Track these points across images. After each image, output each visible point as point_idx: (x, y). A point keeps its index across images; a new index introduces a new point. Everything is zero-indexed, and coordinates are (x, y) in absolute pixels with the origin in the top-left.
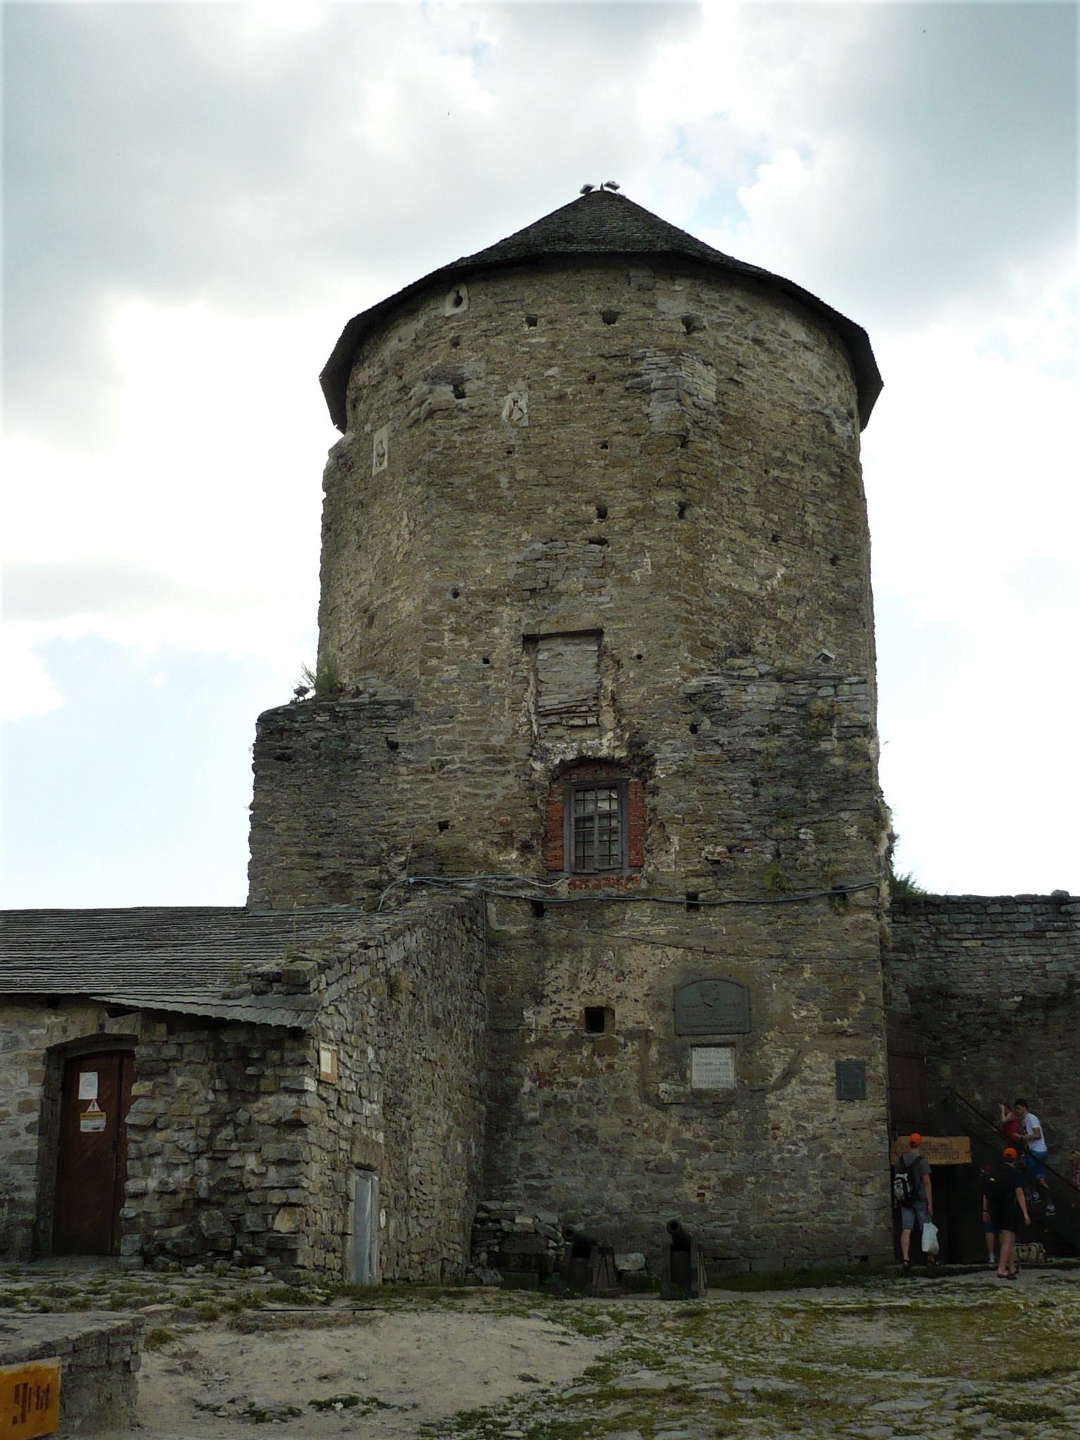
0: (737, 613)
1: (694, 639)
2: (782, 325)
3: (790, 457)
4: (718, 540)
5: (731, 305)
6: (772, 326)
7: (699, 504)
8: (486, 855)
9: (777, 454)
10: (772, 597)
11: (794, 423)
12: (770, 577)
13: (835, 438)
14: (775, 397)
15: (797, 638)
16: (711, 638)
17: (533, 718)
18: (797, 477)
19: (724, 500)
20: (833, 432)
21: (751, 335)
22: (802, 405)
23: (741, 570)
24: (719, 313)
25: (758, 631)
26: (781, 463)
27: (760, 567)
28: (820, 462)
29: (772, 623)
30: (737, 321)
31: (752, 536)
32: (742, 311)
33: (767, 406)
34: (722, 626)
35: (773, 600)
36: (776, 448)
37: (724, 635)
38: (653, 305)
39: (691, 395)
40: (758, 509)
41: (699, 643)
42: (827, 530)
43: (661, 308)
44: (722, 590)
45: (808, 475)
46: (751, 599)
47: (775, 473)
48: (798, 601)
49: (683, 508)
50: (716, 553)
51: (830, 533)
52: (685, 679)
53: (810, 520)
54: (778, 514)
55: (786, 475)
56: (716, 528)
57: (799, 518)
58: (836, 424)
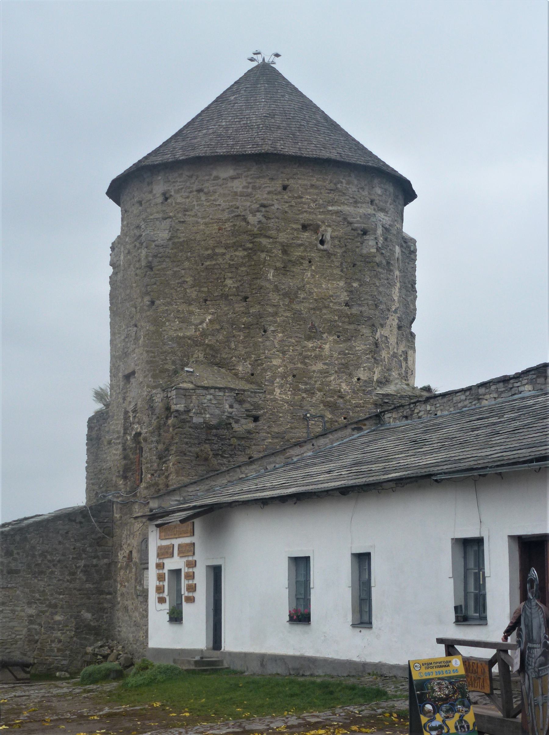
0: (181, 349)
1: (154, 370)
2: (215, 173)
3: (217, 251)
4: (170, 314)
5: (184, 176)
6: (207, 178)
7: (158, 299)
8: (116, 481)
9: (209, 252)
10: (204, 334)
11: (220, 229)
12: (201, 323)
13: (249, 227)
14: (207, 220)
15: (217, 351)
16: (166, 367)
17: (131, 414)
18: (220, 260)
19: (172, 291)
20: (248, 223)
21: (194, 189)
22: (226, 215)
23: (184, 325)
24: (178, 184)
25: (192, 355)
26: (210, 257)
27: (195, 320)
28: (236, 246)
29: (201, 348)
30: (188, 184)
31: (190, 304)
32: (191, 177)
33: (202, 227)
34: (173, 358)
35: (202, 336)
36: (207, 249)
37: (174, 363)
38: (151, 192)
39: (154, 241)
40: (193, 289)
41: (158, 372)
42: (239, 284)
43: (154, 192)
44: (172, 339)
45: (228, 257)
46: (189, 339)
47: (208, 263)
48: (218, 330)
49: (153, 303)
50: (169, 321)
51: (241, 285)
52: (149, 392)
53: (229, 282)
54: (207, 287)
55: (214, 262)
56: (170, 307)
57: (221, 284)
58: (250, 218)
